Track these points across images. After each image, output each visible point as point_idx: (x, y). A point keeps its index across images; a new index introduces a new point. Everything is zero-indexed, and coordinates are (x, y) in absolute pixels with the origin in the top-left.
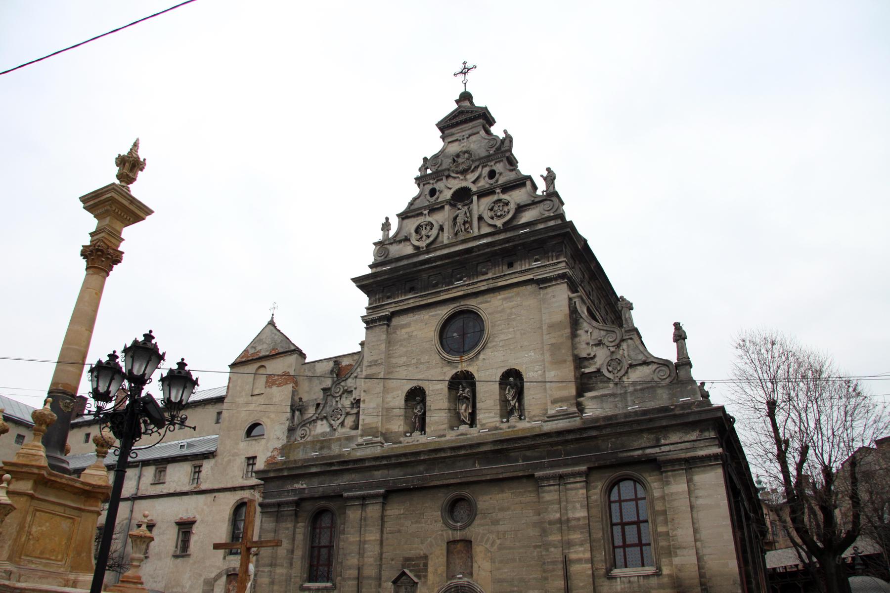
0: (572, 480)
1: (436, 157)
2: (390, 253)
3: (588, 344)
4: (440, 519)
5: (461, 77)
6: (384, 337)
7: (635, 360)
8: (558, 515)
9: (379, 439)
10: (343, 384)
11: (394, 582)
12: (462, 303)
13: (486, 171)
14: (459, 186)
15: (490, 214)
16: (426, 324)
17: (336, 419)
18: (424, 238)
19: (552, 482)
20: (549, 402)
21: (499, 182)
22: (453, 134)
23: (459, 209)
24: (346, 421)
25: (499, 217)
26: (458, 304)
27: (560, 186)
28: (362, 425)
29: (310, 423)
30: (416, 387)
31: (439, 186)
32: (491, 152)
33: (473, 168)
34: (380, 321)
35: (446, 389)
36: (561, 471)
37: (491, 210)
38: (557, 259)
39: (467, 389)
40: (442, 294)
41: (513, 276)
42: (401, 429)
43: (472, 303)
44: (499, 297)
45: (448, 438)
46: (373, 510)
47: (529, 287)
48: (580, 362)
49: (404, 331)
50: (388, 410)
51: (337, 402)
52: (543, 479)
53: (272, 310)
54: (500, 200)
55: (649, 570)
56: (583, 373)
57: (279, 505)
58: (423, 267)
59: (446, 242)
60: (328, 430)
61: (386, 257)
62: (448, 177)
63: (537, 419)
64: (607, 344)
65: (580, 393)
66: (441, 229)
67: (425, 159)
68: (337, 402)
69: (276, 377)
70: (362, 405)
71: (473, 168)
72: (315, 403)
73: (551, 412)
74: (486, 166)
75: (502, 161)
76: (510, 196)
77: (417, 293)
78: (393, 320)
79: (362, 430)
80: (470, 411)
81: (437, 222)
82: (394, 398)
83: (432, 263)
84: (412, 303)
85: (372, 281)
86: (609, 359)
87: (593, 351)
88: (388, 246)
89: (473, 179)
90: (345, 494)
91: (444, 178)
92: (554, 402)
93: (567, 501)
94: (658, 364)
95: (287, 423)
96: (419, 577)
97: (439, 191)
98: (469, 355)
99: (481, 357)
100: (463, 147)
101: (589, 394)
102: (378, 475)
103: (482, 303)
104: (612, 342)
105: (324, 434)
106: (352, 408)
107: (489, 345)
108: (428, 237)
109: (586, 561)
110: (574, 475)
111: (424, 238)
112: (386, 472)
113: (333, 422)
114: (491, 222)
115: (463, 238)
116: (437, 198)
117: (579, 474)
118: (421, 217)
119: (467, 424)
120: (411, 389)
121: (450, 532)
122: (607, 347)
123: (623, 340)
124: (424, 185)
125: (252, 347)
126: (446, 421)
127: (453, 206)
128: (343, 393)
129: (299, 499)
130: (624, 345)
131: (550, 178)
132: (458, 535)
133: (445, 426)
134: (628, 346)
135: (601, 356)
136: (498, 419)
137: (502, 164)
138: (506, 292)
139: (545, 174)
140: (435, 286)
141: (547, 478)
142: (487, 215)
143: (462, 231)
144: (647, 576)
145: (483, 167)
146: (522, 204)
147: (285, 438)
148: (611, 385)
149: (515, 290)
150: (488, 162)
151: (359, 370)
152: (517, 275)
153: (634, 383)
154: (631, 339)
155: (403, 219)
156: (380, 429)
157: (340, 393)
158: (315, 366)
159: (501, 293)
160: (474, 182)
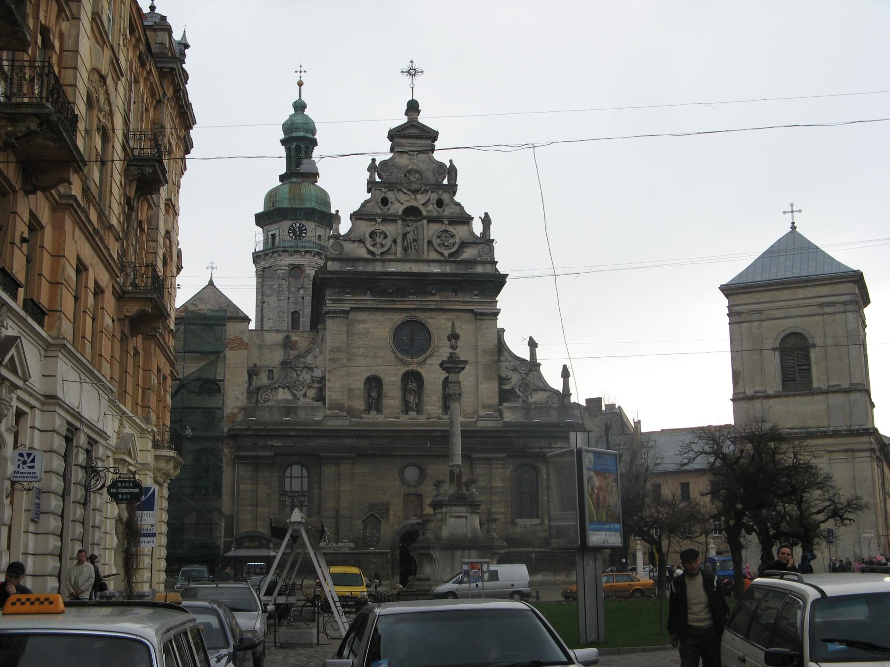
0: (495, 462)
1: (384, 163)
2: (345, 250)
3: (507, 368)
4: (398, 478)
5: (408, 79)
6: (345, 328)
7: (538, 387)
8: (484, 484)
9: (345, 413)
10: (302, 359)
11: (363, 521)
12: (413, 314)
13: (434, 196)
14: (409, 204)
15: (439, 241)
16: (381, 324)
17: (299, 390)
18: (378, 244)
19: (481, 462)
20: (480, 406)
21: (445, 213)
22: (403, 146)
23: (409, 226)
24: (308, 394)
25: (445, 246)
26: (409, 314)
27: (494, 233)
28: (329, 400)
29: (272, 389)
30: (373, 376)
31: (391, 196)
32: (440, 180)
33: (423, 190)
34: (340, 314)
35: (400, 382)
36: (489, 455)
37: (439, 237)
38: (491, 299)
39: (415, 384)
40: (397, 303)
41: (457, 303)
42: (363, 407)
43: (421, 316)
44: (444, 317)
45: (401, 420)
46: (345, 469)
47: (467, 315)
48: (502, 380)
49: (361, 326)
50: (350, 391)
51: (298, 375)
52: (477, 459)
53: (210, 270)
54: (446, 231)
55: (537, 521)
56: (502, 389)
57: (256, 457)
58: (384, 277)
59: (399, 255)
60: (290, 398)
61: (340, 253)
62: (399, 190)
63: (469, 416)
64: (521, 371)
65: (500, 404)
66: (395, 242)
67: (374, 160)
68: (298, 375)
69: (227, 341)
70: (328, 385)
71: (423, 190)
72: (268, 369)
73: (481, 413)
74: (434, 192)
75: (449, 192)
76: (455, 229)
77: (375, 296)
78: (351, 313)
79: (330, 404)
80: (417, 401)
81: (390, 233)
82: (355, 381)
83: (392, 276)
84: (370, 304)
85: (335, 276)
86: (520, 382)
87: (510, 374)
88: (341, 241)
89: (423, 202)
90: (321, 455)
91: (395, 190)
92: (484, 407)
93: (491, 475)
94: (552, 392)
95: (246, 386)
96: (383, 518)
97: (391, 202)
98: (419, 359)
99: (428, 362)
100: (413, 163)
101: (505, 404)
102: (348, 442)
103: (429, 318)
104: (524, 370)
105: (286, 401)
106: (313, 381)
107: (435, 354)
108: (382, 246)
109: (502, 513)
110: (497, 459)
111: (378, 244)
112: (355, 440)
113: (295, 392)
114: (438, 249)
115: (414, 257)
116: (389, 209)
117: (501, 459)
118: (374, 223)
119: (414, 410)
120: (369, 377)
121: (406, 488)
122: (520, 373)
123: (531, 371)
124: (375, 190)
125: (192, 304)
126: (400, 407)
127: (403, 220)
128: (304, 368)
129: (276, 455)
130: (531, 374)
131: (486, 221)
132: (412, 490)
133: (399, 411)
134: (534, 375)
135: (515, 378)
136: (440, 411)
137: (448, 194)
138: (449, 314)
139: (483, 216)
140: (390, 294)
141: (480, 459)
142: (436, 242)
143: (411, 248)
144: (536, 525)
145: (432, 192)
146: (466, 241)
147: (245, 399)
148: (520, 400)
149: (457, 314)
150: (437, 189)
151: (317, 350)
152: (460, 303)
153: (535, 403)
154: (536, 371)
155: (356, 219)
156: (346, 406)
157: (300, 369)
158: (263, 334)
159: (445, 314)
160: (423, 205)
